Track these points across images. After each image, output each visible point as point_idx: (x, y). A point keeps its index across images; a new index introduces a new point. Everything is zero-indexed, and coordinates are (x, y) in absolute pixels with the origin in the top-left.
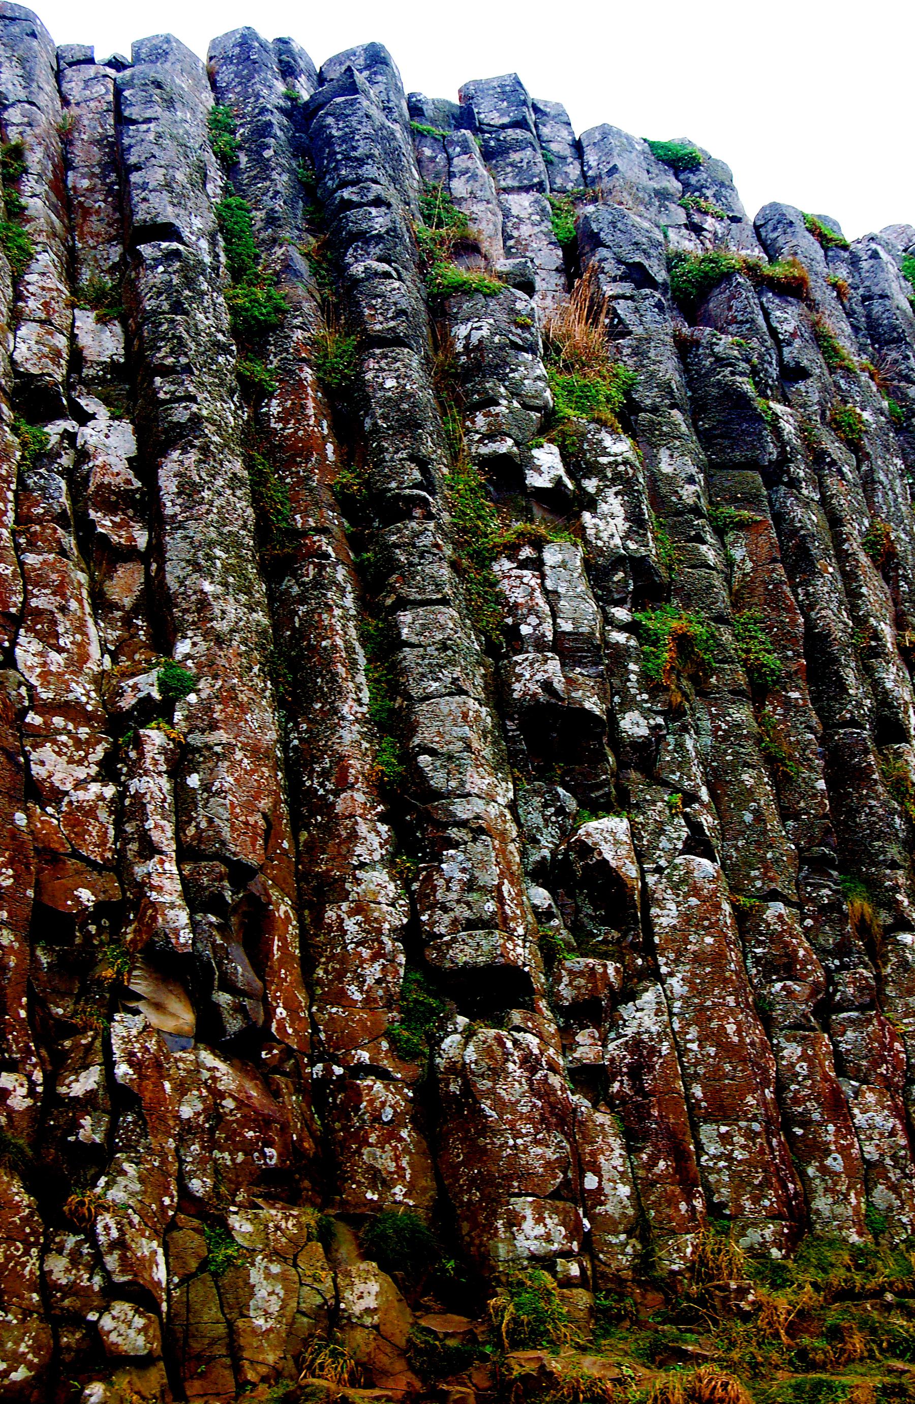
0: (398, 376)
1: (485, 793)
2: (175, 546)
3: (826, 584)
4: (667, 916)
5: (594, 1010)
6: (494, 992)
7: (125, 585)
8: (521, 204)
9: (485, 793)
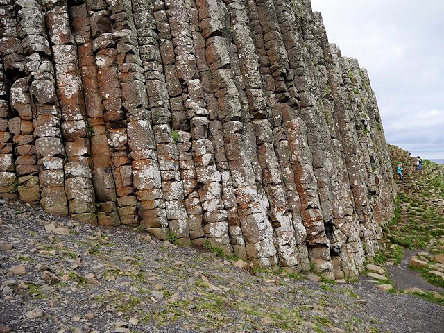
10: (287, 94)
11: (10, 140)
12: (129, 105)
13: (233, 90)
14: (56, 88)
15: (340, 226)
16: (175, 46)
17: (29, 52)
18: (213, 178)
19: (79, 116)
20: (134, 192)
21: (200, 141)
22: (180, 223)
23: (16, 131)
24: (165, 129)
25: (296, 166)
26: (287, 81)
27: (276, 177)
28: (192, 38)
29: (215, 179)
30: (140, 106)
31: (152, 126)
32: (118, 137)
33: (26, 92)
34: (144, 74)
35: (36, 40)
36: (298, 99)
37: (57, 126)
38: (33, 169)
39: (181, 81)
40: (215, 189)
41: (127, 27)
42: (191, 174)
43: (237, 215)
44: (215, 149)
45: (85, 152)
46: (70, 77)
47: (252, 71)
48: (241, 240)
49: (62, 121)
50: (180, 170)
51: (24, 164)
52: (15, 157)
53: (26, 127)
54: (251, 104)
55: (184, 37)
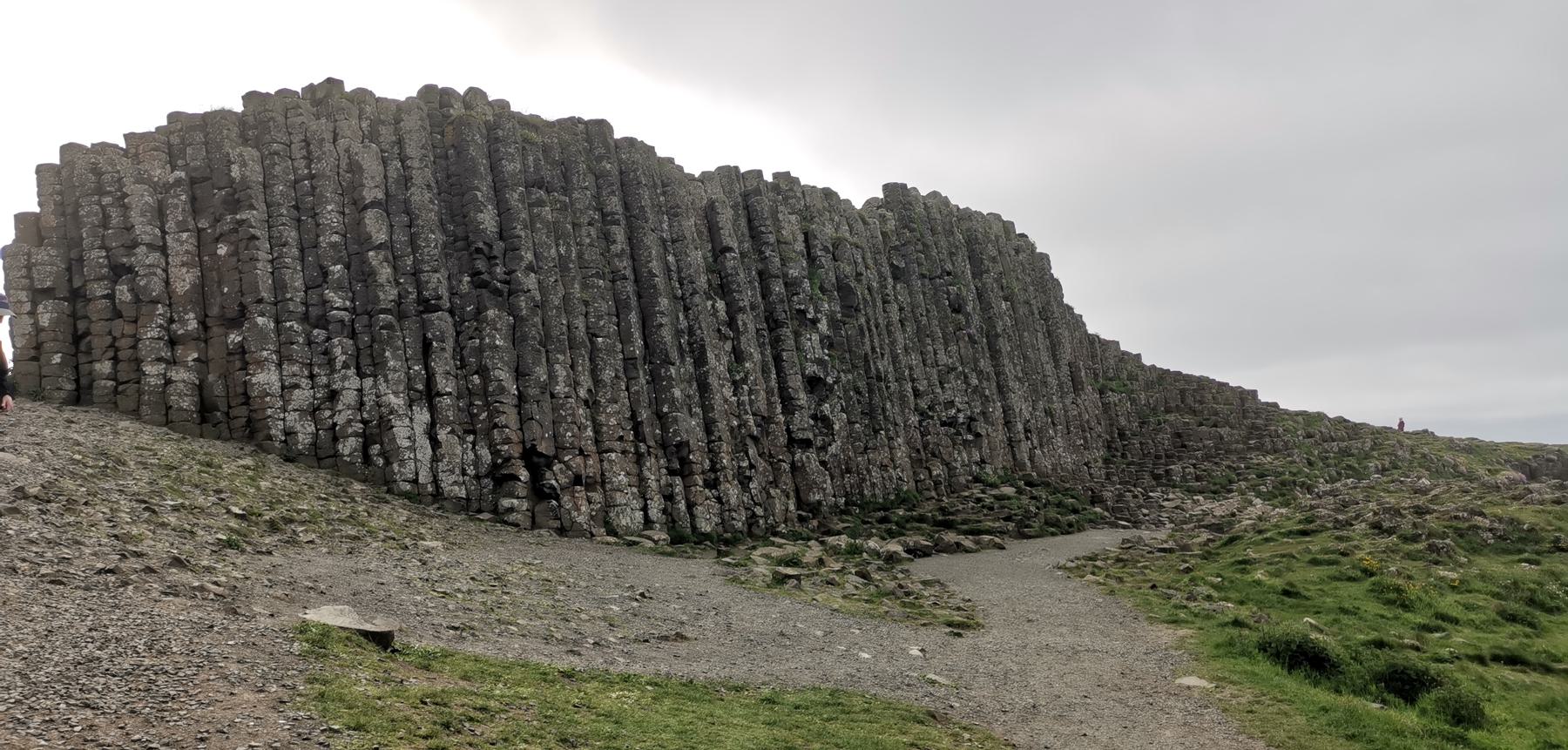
0: (778, 288)
1: (802, 398)
2: (743, 339)
3: (867, 340)
4: (836, 427)
5: (823, 448)
6: (806, 444)
7: (728, 346)
8: (793, 218)
9: (802, 398)
10: (485, 277)
11: (112, 346)
12: (248, 300)
13: (385, 272)
14: (167, 283)
17: (135, 245)
18: (346, 384)
19: (192, 315)
20: (247, 399)
21: (336, 341)
22: (301, 437)
23: (117, 334)
25: (483, 371)
26: (491, 258)
27: (445, 385)
28: (343, 213)
29: (350, 385)
30: (260, 301)
31: (277, 322)
32: (234, 338)
33: (131, 290)
34: (272, 262)
35: (145, 230)
36: (507, 282)
37: (161, 326)
38: (133, 376)
39: (322, 267)
40: (349, 397)
41: (252, 207)
42: (324, 380)
43: (376, 431)
44: (358, 349)
45: (196, 355)
46: (184, 270)
48: (381, 462)
49: (171, 321)
50: (312, 377)
51: (125, 371)
52: (115, 360)
53: (129, 329)
54: (419, 293)
55: (330, 214)
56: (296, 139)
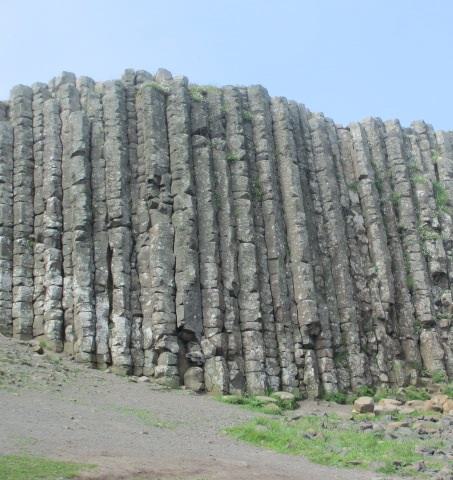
15: (210, 335)
16: (43, 170)
24: (21, 242)
39: (44, 200)
47: (114, 183)
56: (36, 113)
